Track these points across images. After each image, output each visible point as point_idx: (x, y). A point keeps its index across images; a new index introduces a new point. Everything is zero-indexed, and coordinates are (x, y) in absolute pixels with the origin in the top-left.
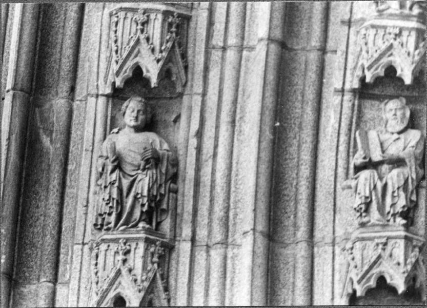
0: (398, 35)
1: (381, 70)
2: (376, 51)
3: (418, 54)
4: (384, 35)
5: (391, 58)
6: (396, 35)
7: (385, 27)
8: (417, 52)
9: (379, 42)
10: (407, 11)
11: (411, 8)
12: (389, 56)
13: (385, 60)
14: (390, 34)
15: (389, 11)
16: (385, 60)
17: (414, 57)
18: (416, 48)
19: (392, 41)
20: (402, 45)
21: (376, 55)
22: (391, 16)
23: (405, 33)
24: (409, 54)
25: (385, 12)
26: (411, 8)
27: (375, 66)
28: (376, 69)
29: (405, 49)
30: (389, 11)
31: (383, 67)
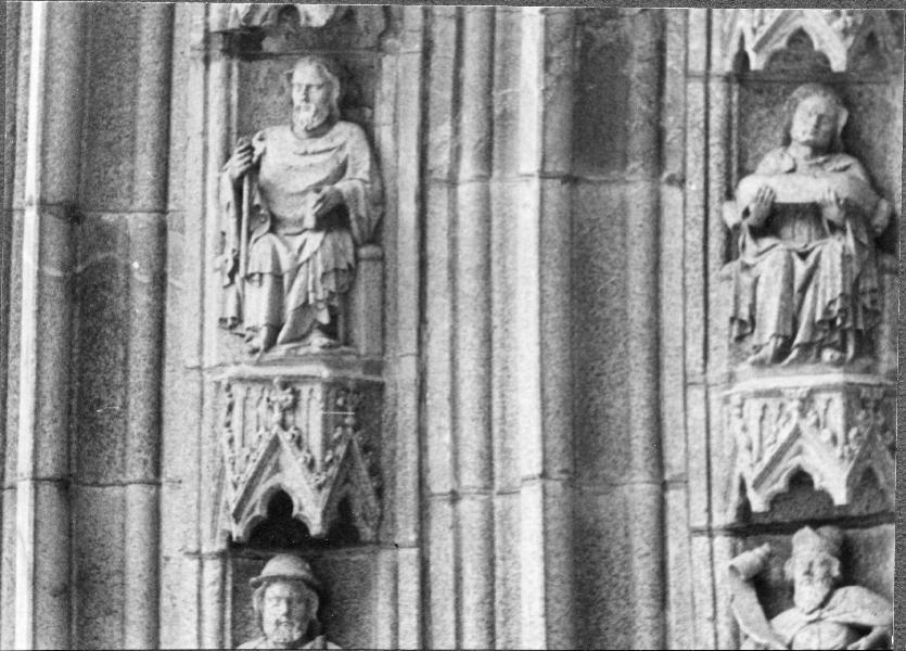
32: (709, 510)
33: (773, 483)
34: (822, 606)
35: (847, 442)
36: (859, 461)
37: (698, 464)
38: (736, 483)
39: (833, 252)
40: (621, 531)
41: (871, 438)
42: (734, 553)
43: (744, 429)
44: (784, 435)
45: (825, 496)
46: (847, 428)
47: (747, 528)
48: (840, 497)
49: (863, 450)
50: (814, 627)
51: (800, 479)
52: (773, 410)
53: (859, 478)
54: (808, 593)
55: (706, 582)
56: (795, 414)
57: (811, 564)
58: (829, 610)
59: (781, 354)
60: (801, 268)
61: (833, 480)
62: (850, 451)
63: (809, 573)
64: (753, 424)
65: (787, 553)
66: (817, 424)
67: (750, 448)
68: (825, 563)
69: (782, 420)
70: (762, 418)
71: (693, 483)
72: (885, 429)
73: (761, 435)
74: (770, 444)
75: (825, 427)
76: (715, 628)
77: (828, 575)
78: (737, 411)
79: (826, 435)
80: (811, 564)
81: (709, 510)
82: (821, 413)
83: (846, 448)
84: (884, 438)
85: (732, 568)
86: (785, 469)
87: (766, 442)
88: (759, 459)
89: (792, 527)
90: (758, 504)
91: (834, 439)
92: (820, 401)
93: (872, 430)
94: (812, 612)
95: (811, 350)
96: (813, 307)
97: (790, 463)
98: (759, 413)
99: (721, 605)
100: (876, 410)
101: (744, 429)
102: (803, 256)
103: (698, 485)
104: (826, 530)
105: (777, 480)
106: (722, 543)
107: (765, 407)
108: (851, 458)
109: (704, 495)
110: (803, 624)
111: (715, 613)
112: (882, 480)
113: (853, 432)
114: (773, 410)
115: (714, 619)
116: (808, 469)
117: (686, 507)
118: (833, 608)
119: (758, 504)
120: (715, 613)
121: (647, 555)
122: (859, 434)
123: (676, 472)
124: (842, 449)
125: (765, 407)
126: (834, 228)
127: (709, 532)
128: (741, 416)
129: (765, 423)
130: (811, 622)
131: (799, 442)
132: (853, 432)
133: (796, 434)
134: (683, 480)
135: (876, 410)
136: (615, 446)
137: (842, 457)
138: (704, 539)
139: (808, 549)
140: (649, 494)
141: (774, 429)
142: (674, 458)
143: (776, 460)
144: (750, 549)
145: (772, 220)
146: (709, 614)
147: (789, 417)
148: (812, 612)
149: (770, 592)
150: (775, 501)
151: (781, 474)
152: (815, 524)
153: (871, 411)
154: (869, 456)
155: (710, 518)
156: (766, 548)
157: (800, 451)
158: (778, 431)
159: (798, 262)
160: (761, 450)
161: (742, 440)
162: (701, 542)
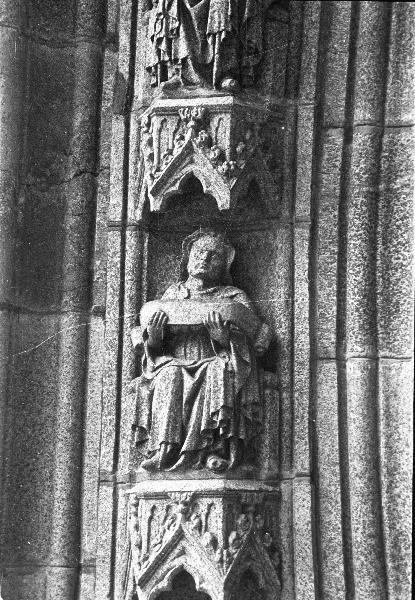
33: (157, 583)
35: (226, 546)
36: (238, 563)
37: (104, 553)
39: (217, 368)
41: (251, 539)
43: (137, 527)
44: (169, 536)
46: (226, 535)
49: (242, 553)
52: (160, 513)
56: (180, 516)
59: (169, 460)
60: (189, 382)
64: (144, 525)
66: (199, 527)
67: (140, 546)
69: (168, 521)
70: (151, 518)
72: (264, 530)
73: (149, 535)
75: (206, 531)
78: (134, 509)
79: (206, 538)
82: (203, 518)
83: (225, 552)
84: (263, 540)
86: (168, 570)
87: (152, 543)
88: (146, 558)
91: (214, 542)
92: (203, 508)
95: (194, 461)
96: (198, 419)
97: (173, 563)
98: (149, 514)
100: (255, 514)
101: (137, 527)
102: (192, 372)
103: (103, 569)
107: (154, 508)
108: (229, 563)
109: (107, 582)
113: (233, 535)
114: (160, 513)
116: (190, 570)
122: (238, 537)
123: (88, 557)
125: (154, 508)
126: (221, 348)
128: (136, 515)
131: (183, 543)
132: (233, 535)
134: (91, 567)
135: (255, 514)
136: (41, 532)
137: (221, 561)
140: (63, 578)
141: (161, 530)
142: (87, 545)
143: (161, 559)
145: (167, 340)
147: (174, 519)
151: (166, 573)
153: (251, 517)
154: (249, 558)
157: (183, 552)
158: (164, 531)
159: (186, 377)
161: (134, 539)
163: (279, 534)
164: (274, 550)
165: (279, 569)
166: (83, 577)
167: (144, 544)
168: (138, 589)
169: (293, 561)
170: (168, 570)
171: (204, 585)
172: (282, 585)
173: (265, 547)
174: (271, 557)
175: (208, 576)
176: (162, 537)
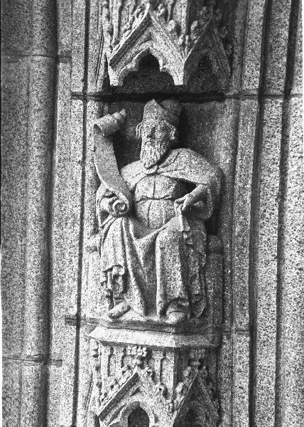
0: (146, 360)
1: (123, 417)
2: (112, 387)
3: (182, 392)
4: (123, 357)
5: (137, 398)
6: (142, 359)
7: (124, 346)
8: (179, 389)
9: (117, 370)
10: (156, 318)
11: (163, 313)
12: (134, 394)
13: (128, 401)
14: (133, 356)
15: (128, 317)
16: (128, 401)
17: (175, 397)
18: (178, 378)
19: (136, 370)
20: (153, 377)
21: (112, 394)
22: (133, 325)
23: (158, 356)
24: (166, 394)
25: (122, 318)
26: (163, 313)
27: (113, 412)
28: (115, 416)
29: (158, 385)
30: (128, 317)
31: (125, 412)
32: (85, 80)
33: (126, 64)
34: (159, 163)
35: (188, 32)
36: (197, 50)
38: (103, 61)
40: (24, 91)
41: (209, 32)
42: (101, 114)
43: (109, 17)
44: (138, 22)
45: (167, 76)
46: (189, 23)
47: (109, 98)
48: (178, 80)
50: (152, 178)
51: (149, 61)
53: (196, 65)
54: (149, 152)
55: (79, 135)
57: (154, 130)
58: (164, 167)
61: (175, 64)
62: (190, 40)
63: (152, 136)
64: (115, 13)
65: (139, 118)
66: (165, 15)
67: (111, 33)
68: (165, 129)
69: (138, 10)
71: (74, 58)
72: (221, 24)
73: (120, 22)
74: (126, 31)
76: (83, 169)
77: (166, 138)
79: (171, 25)
80: (154, 130)
81: (85, 80)
82: (169, 7)
84: (220, 31)
85: (96, 126)
86: (136, 53)
87: (123, 29)
88: (117, 42)
89: (145, 98)
90: (114, 80)
91: (178, 29)
93: (211, 24)
94: (152, 167)
99: (89, 153)
100: (215, 8)
103: (78, 60)
104: (168, 104)
105: (130, 61)
106: (92, 106)
108: (190, 47)
110: (142, 175)
111: (84, 158)
112: (215, 67)
113: (195, 24)
115: (83, 163)
116: (155, 54)
117: (71, 77)
118: (167, 165)
119: (114, 80)
120: (84, 158)
121: (39, 110)
122: (199, 26)
124: (184, 38)
127: (84, 97)
128: (107, 7)
129: (124, 13)
130: (149, 175)
131: (150, 30)
132: (195, 24)
133: (148, 23)
134: (68, 57)
135: (215, 8)
137: (183, 45)
138: (80, 102)
139: (152, 118)
141: (131, 18)
142: (64, 40)
143: (131, 43)
144: (111, 113)
146: (80, 158)
147: (143, 9)
148: (152, 167)
149: (124, 148)
150: (129, 77)
152: (160, 97)
154: (206, 46)
155: (85, 88)
156: (123, 112)
157: (150, 38)
158: (134, 19)
160: (119, 35)
161: (106, 26)
162: (78, 103)
163: (233, 29)
164: (227, 41)
165: (231, 59)
166: (61, 65)
167: (116, 30)
168: (110, 70)
169: (243, 53)
170: (136, 53)
171: (166, 66)
172: (231, 73)
173: (220, 37)
174: (225, 48)
175: (171, 59)
176: (131, 24)
